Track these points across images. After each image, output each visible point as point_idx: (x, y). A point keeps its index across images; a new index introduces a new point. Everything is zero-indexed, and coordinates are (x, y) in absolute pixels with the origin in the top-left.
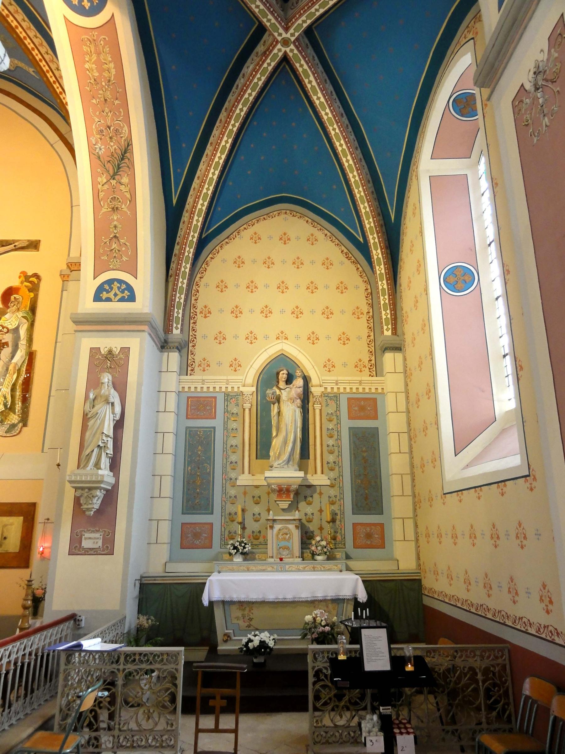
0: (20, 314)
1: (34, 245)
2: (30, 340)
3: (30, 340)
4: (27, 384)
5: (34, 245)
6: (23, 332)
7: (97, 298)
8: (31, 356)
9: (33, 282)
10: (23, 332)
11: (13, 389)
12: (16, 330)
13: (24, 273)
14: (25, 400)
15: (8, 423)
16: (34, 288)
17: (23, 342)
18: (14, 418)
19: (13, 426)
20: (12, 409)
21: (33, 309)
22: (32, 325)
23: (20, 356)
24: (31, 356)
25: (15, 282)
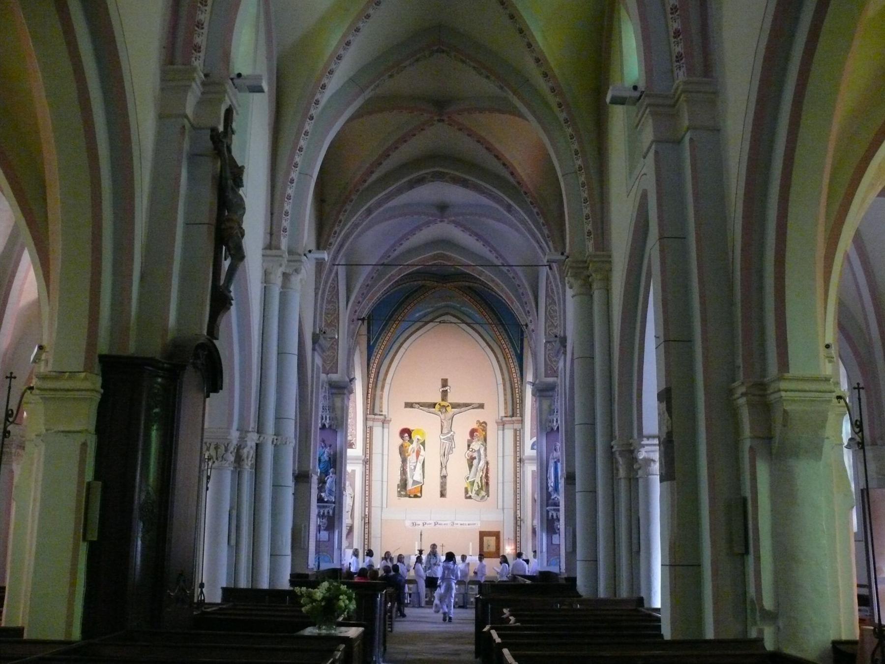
0: (480, 443)
1: (481, 406)
2: (486, 456)
3: (486, 456)
4: (487, 477)
5: (481, 406)
6: (482, 451)
7: (532, 448)
8: (487, 463)
9: (483, 425)
10: (482, 451)
11: (481, 480)
12: (479, 451)
13: (478, 421)
14: (487, 484)
15: (481, 495)
16: (485, 430)
17: (483, 456)
18: (483, 493)
19: (483, 497)
20: (482, 489)
21: (485, 440)
22: (486, 449)
23: (482, 463)
24: (487, 463)
25: (475, 426)
